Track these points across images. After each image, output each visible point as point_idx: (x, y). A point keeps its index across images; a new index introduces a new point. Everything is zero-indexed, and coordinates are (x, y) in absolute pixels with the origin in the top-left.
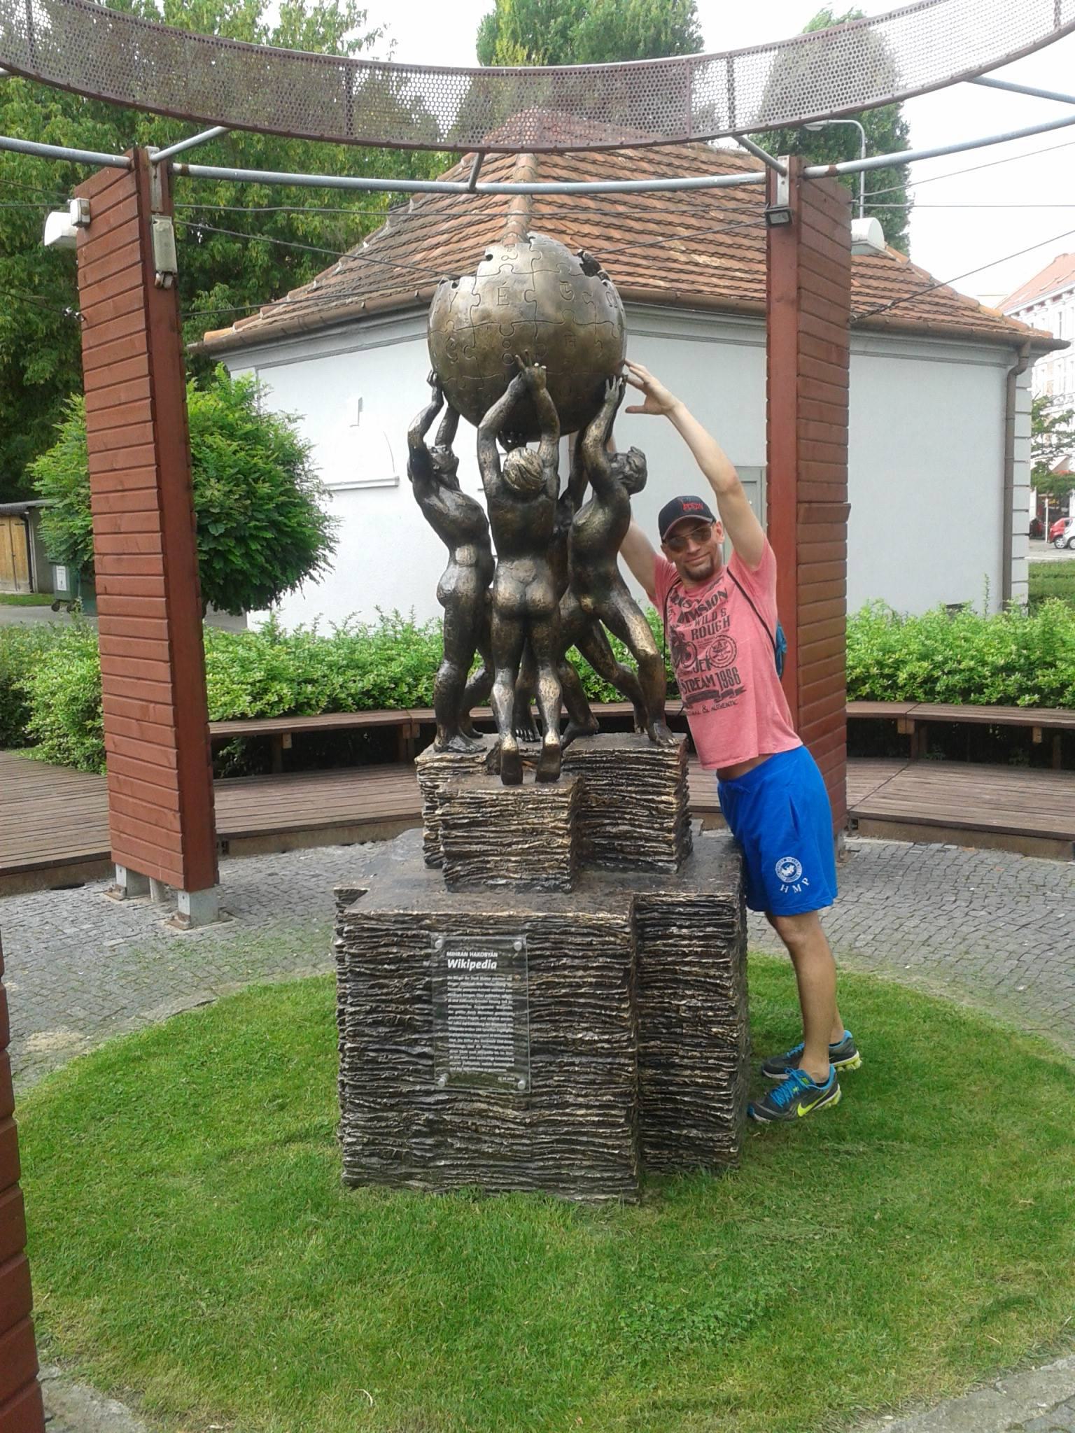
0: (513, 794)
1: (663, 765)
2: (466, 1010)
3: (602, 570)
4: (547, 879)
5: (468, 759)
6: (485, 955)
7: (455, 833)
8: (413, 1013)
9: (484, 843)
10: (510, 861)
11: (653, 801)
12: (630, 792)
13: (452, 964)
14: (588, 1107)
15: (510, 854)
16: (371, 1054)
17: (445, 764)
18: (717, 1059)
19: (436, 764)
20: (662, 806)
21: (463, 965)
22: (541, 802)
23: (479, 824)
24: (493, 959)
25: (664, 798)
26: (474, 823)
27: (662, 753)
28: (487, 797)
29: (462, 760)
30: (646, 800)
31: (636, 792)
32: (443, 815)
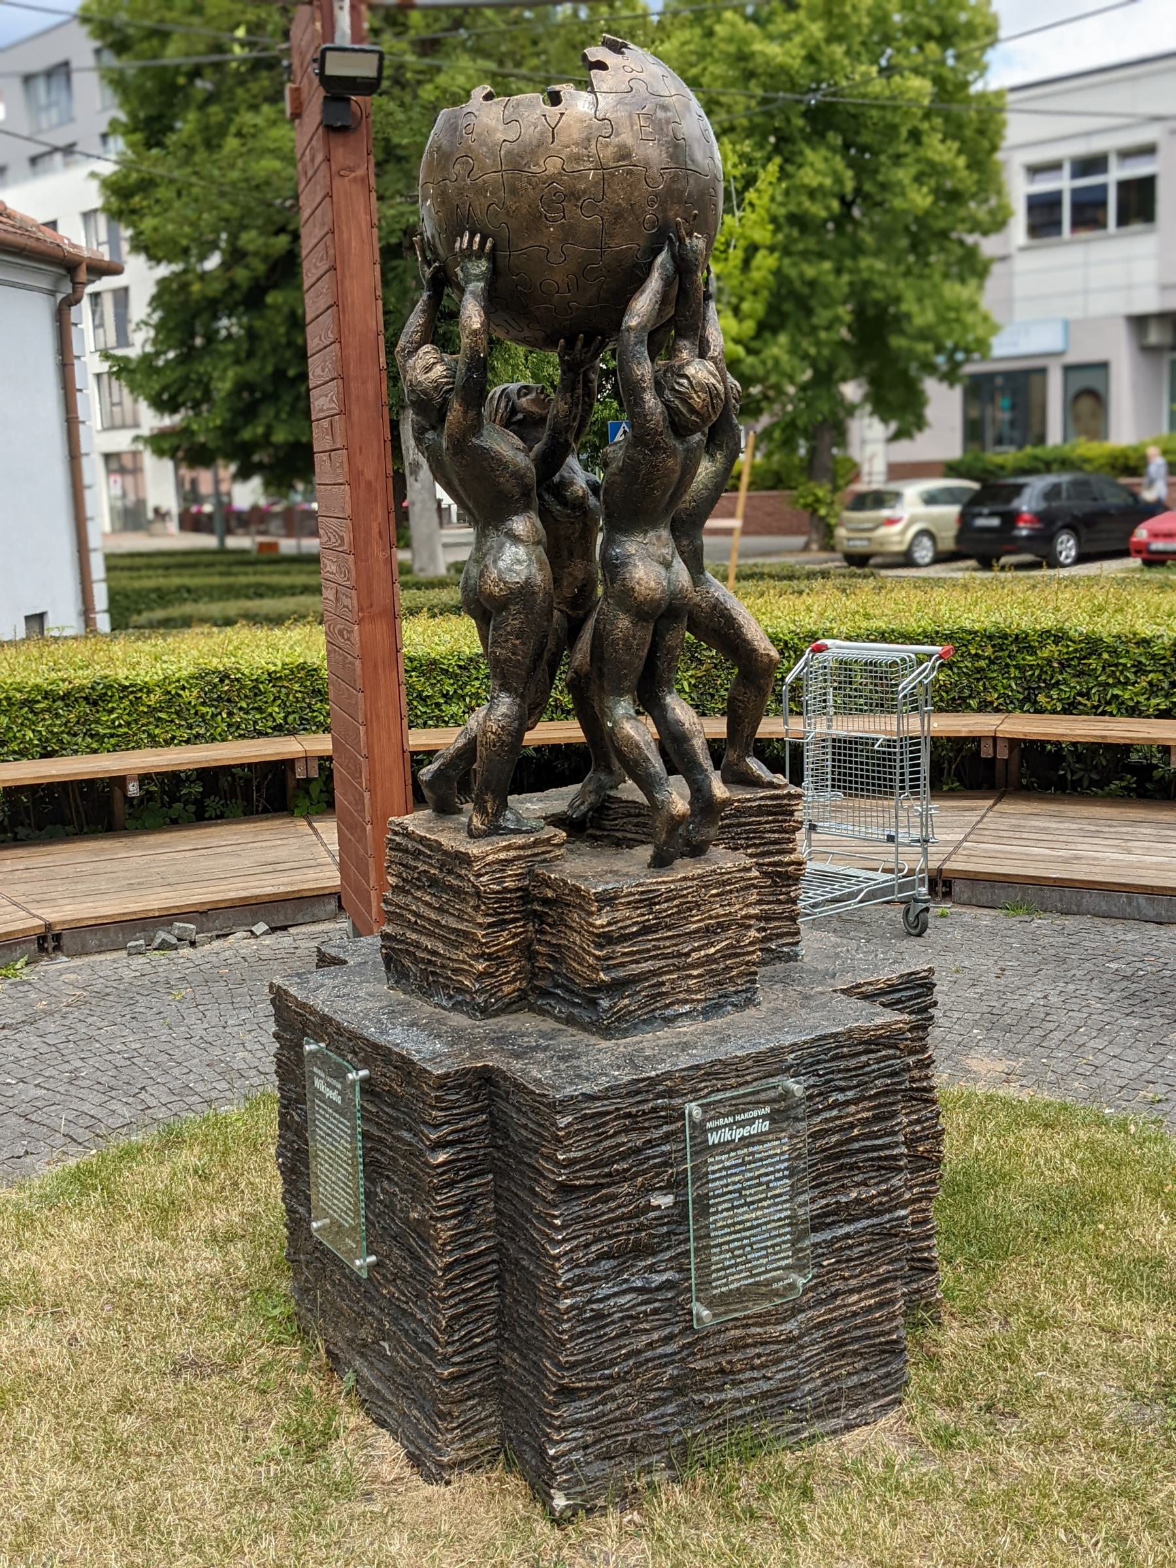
2: (731, 1200)
4: (736, 993)
6: (755, 1114)
8: (650, 1227)
10: (690, 976)
13: (713, 1139)
14: (859, 1290)
15: (693, 966)
16: (594, 1306)
17: (512, 853)
18: (923, 1184)
19: (502, 856)
21: (726, 1135)
22: (724, 883)
24: (764, 1117)
26: (646, 930)
28: (663, 888)
29: (536, 844)
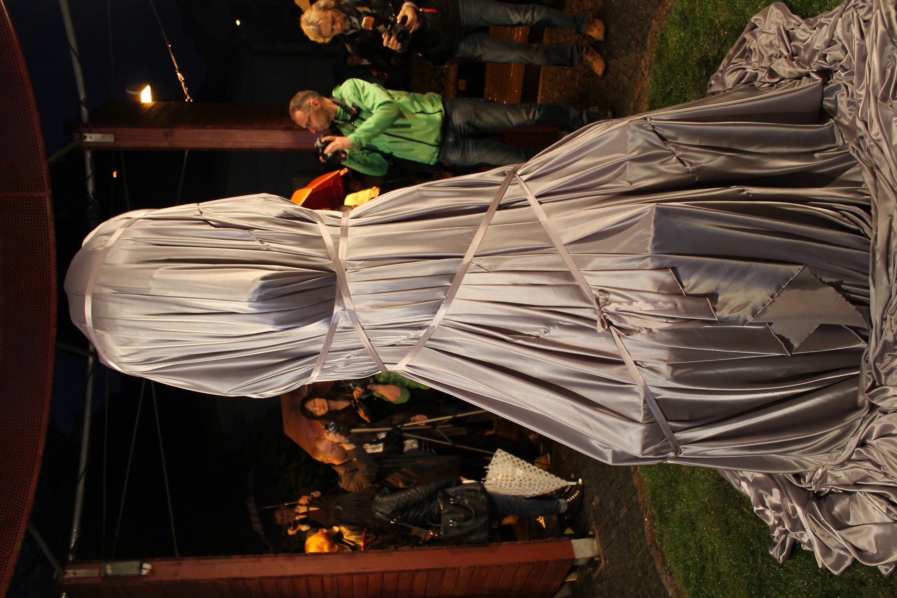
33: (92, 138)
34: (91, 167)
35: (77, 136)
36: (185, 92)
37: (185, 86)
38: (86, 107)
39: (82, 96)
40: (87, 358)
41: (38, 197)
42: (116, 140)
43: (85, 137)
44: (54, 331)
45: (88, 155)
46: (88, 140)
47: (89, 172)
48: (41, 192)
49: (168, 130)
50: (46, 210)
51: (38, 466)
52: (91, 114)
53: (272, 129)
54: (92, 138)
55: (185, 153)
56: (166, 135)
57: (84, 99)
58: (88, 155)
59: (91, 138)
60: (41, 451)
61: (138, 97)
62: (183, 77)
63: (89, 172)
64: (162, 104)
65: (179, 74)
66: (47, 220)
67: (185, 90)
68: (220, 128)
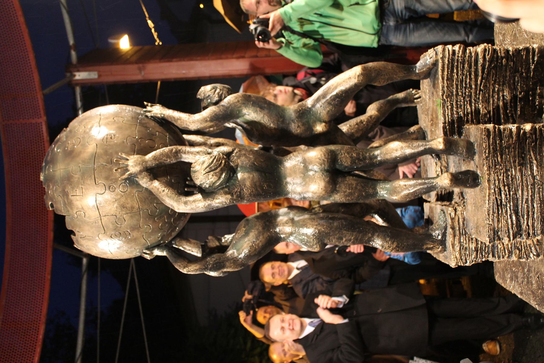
0: (489, 174)
1: (453, 60)
3: (293, 115)
5: (453, 222)
7: (524, 227)
9: (532, 200)
11: (483, 66)
12: (476, 85)
17: (456, 242)
20: (487, 58)
23: (516, 206)
25: (480, 56)
27: (443, 58)
28: (493, 198)
30: (483, 72)
31: (476, 81)
32: (509, 237)
33: (80, 76)
34: (81, 101)
35: (68, 74)
36: (156, 37)
37: (155, 31)
38: (74, 50)
39: (71, 42)
40: (81, 260)
41: (36, 123)
42: (100, 76)
43: (75, 76)
44: (51, 235)
45: (78, 90)
46: (77, 77)
47: (79, 104)
48: (38, 118)
49: (141, 65)
50: (43, 134)
51: (38, 350)
52: (79, 58)
53: (227, 58)
54: (80, 76)
55: (157, 83)
56: (140, 69)
57: (73, 44)
58: (78, 90)
59: (79, 76)
60: (41, 337)
61: (118, 44)
62: (153, 23)
63: (79, 104)
64: (136, 48)
65: (149, 22)
66: (44, 142)
67: (155, 35)
68: (184, 60)
